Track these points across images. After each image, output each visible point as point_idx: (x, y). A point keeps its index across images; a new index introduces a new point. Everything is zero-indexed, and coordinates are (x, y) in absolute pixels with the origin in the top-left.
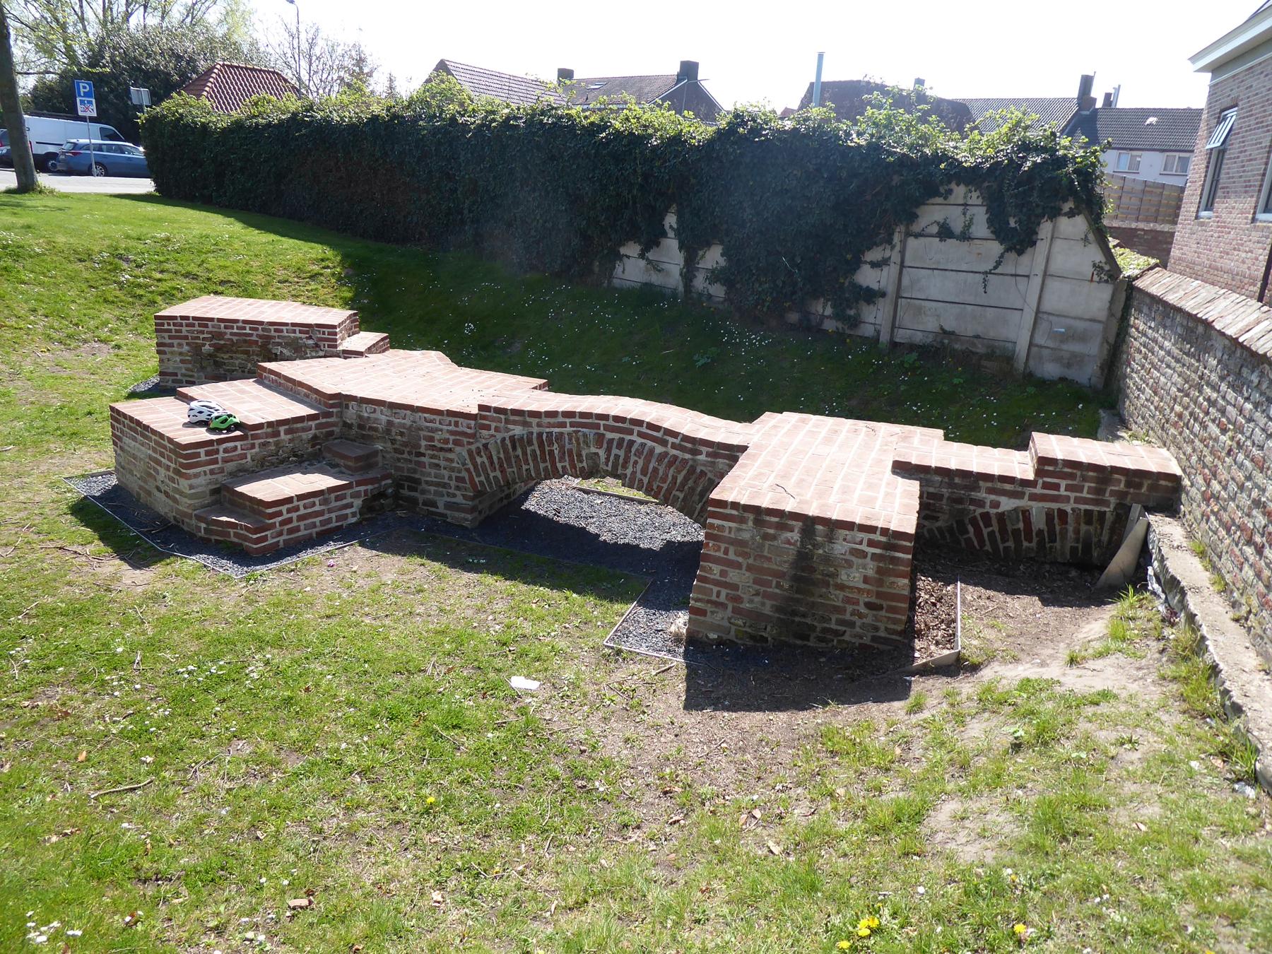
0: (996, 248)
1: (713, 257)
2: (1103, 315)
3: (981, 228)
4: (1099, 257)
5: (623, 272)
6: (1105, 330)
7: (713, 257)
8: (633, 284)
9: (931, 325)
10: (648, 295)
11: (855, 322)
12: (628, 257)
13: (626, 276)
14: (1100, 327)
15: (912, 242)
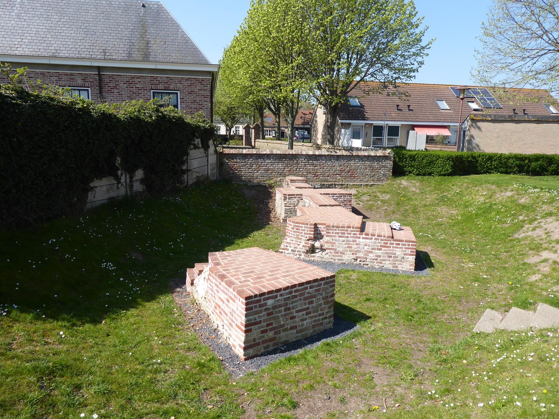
0: (202, 150)
1: (139, 174)
2: (216, 162)
3: (200, 146)
4: (214, 149)
5: (94, 197)
6: (217, 166)
7: (139, 174)
8: (103, 202)
9: (195, 176)
10: (112, 202)
11: (181, 182)
12: (96, 187)
13: (96, 200)
14: (216, 165)
15: (191, 151)
